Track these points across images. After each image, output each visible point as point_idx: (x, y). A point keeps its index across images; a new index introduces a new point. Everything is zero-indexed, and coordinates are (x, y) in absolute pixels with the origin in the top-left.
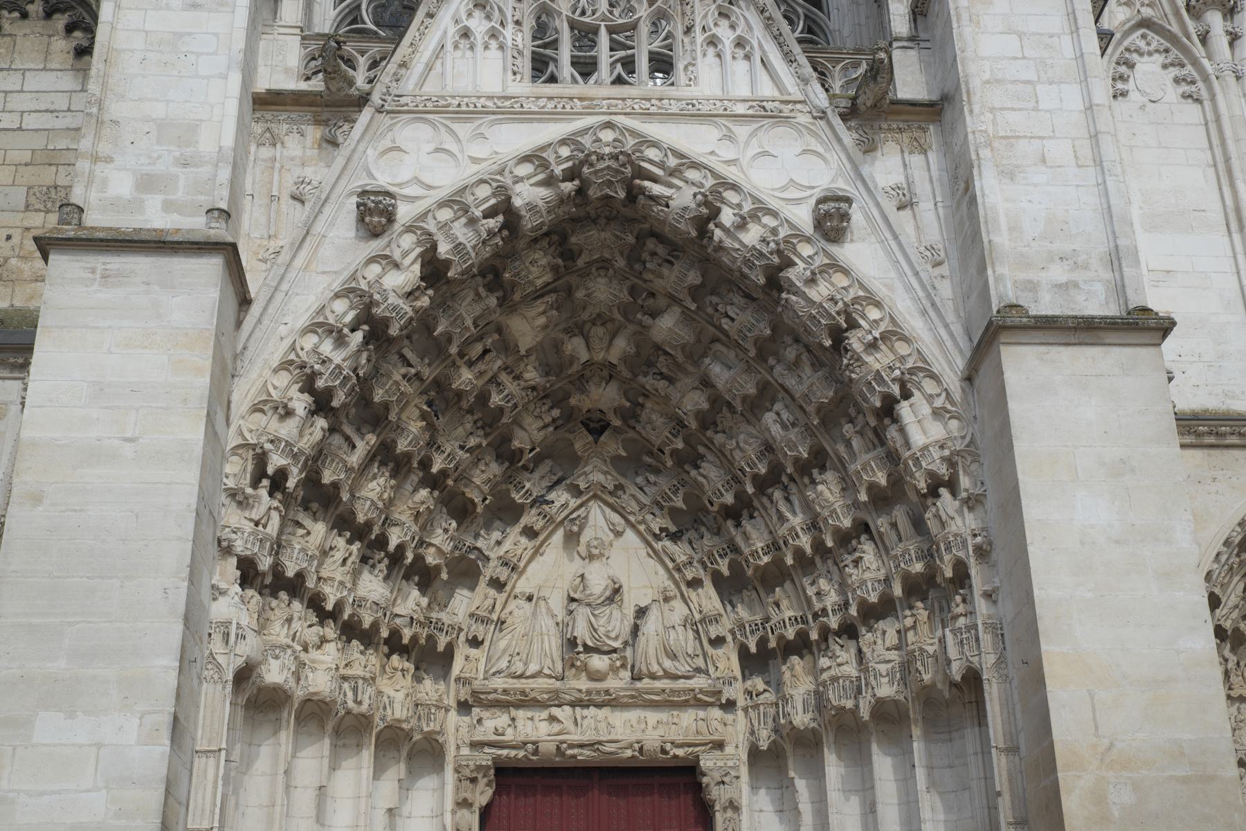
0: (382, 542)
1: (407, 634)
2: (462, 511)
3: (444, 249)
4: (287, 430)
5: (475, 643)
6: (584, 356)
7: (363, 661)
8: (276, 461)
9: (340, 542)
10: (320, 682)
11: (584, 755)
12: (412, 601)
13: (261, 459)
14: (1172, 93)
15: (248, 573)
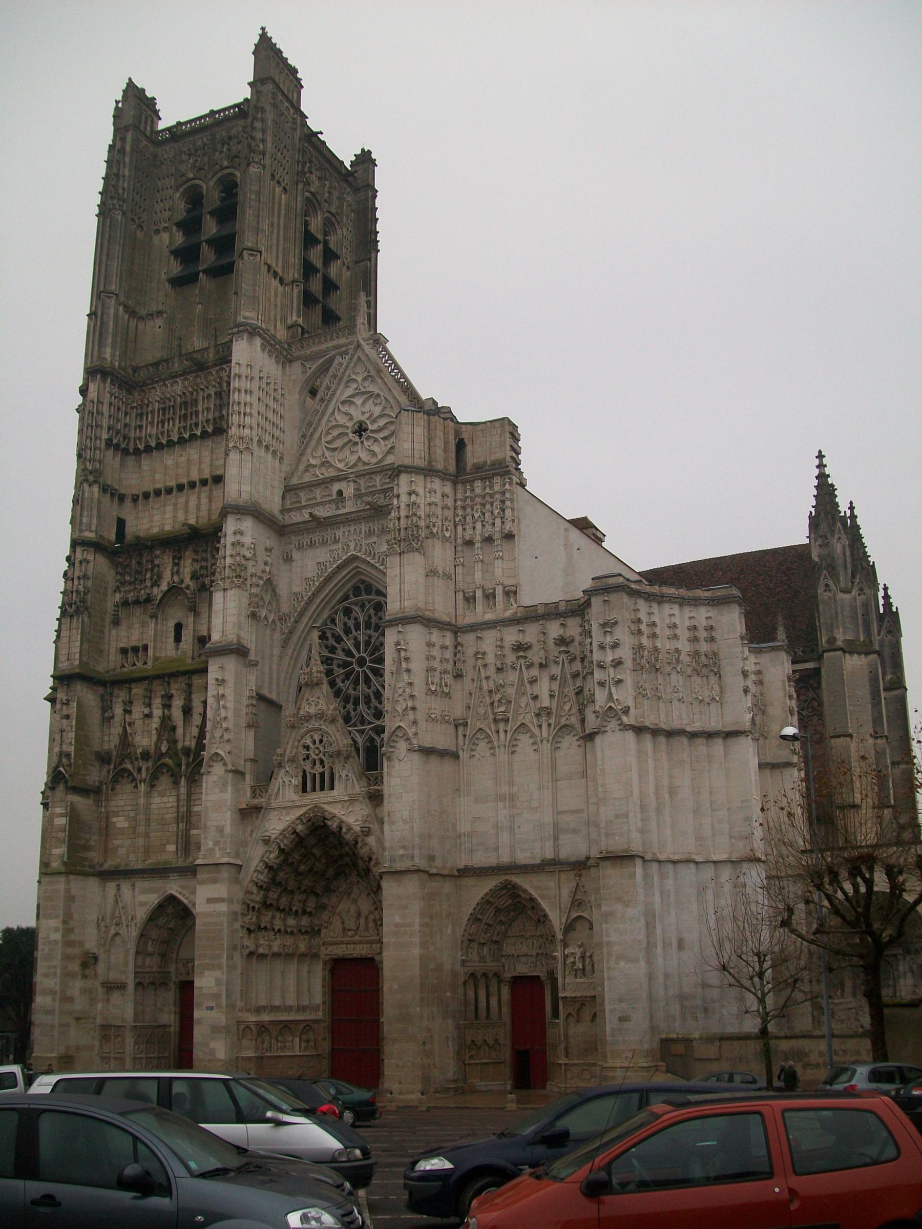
0: (291, 910)
1: (303, 930)
2: (317, 895)
3: (282, 846)
4: (253, 897)
5: (325, 928)
6: (337, 853)
7: (289, 940)
8: (252, 905)
9: (278, 914)
10: (276, 949)
11: (349, 957)
12: (305, 921)
13: (248, 905)
14: (488, 754)
15: (250, 931)
